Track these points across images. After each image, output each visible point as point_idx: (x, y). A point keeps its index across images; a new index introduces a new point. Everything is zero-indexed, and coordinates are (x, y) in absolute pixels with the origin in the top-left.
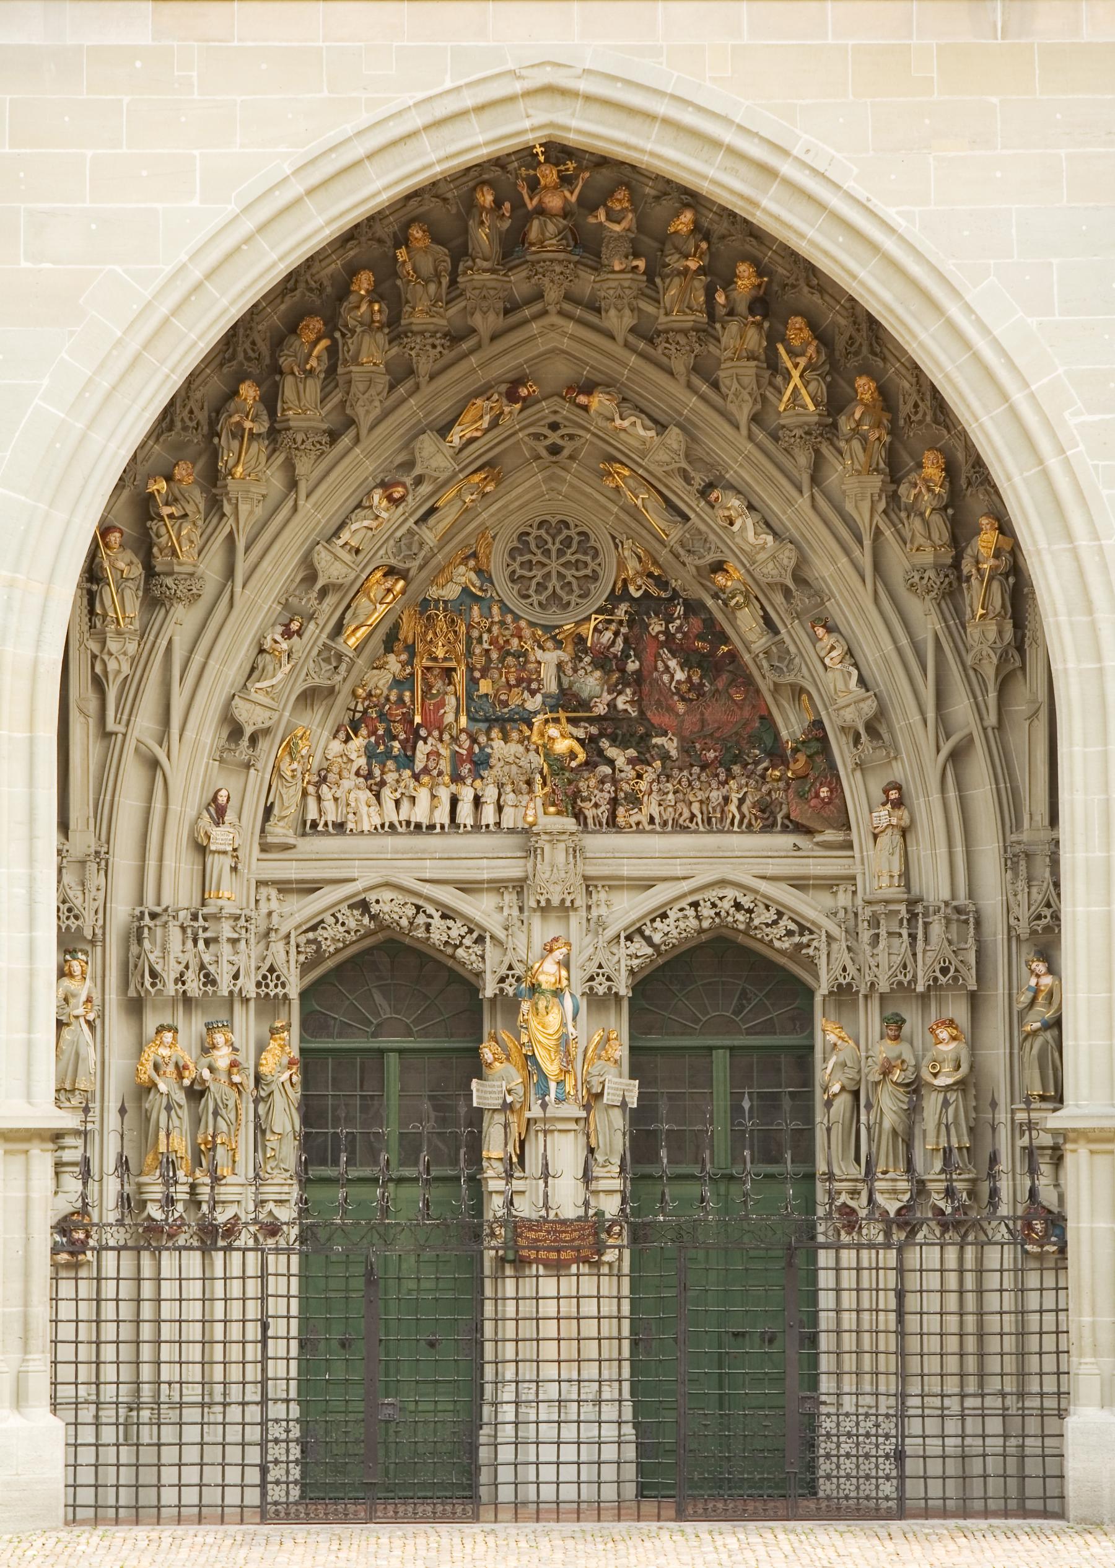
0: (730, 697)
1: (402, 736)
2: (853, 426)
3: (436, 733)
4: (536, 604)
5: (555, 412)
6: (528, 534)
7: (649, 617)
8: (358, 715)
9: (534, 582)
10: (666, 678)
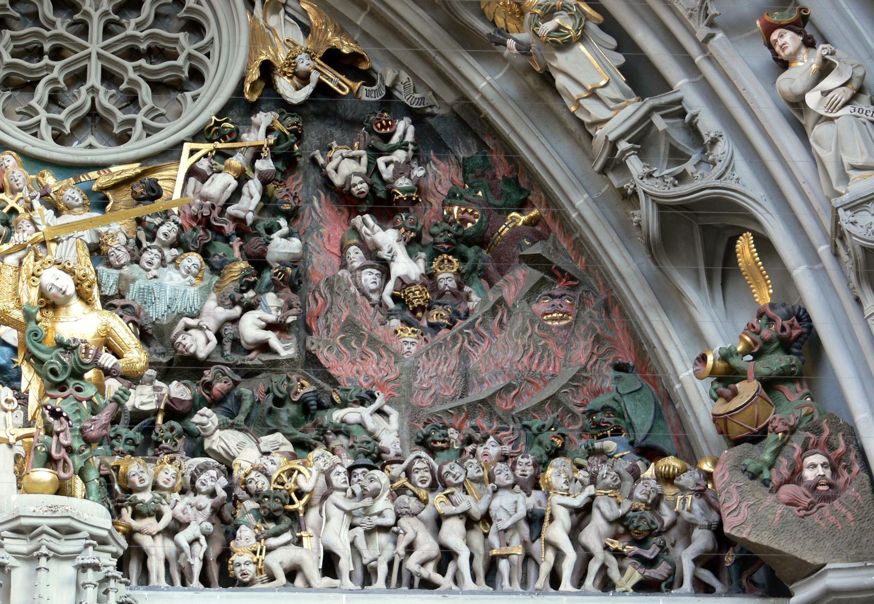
4: (46, 131)
9: (42, 91)
10: (369, 278)
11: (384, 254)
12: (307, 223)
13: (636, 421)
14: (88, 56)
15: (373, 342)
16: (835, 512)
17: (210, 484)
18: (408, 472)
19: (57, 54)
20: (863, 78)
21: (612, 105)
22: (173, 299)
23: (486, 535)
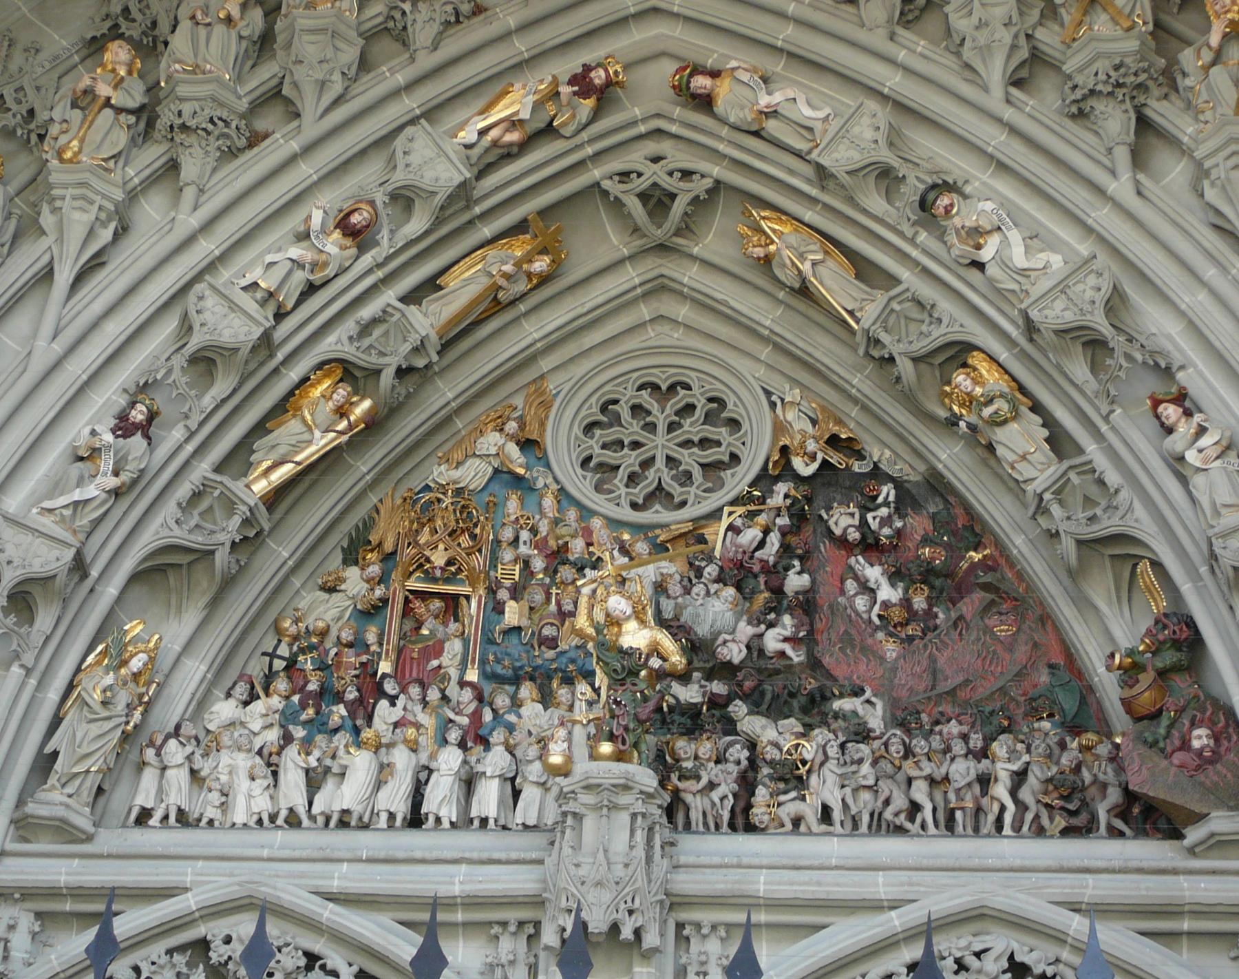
0: (988, 630)
1: (351, 694)
2: (1207, 56)
3: (415, 690)
4: (625, 503)
5: (659, 132)
6: (616, 402)
7: (829, 508)
8: (279, 664)
9: (622, 474)
10: (861, 603)
11: (872, 585)
12: (816, 563)
13: (1066, 707)
14: (656, 447)
15: (865, 649)
16: (1218, 773)
17: (736, 755)
18: (886, 745)
19: (636, 445)
20: (1231, 437)
21: (1039, 467)
22: (714, 621)
23: (946, 792)
